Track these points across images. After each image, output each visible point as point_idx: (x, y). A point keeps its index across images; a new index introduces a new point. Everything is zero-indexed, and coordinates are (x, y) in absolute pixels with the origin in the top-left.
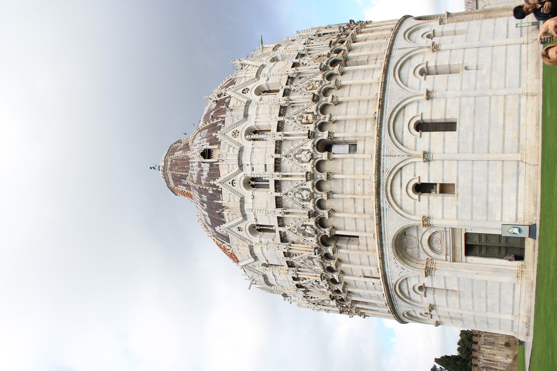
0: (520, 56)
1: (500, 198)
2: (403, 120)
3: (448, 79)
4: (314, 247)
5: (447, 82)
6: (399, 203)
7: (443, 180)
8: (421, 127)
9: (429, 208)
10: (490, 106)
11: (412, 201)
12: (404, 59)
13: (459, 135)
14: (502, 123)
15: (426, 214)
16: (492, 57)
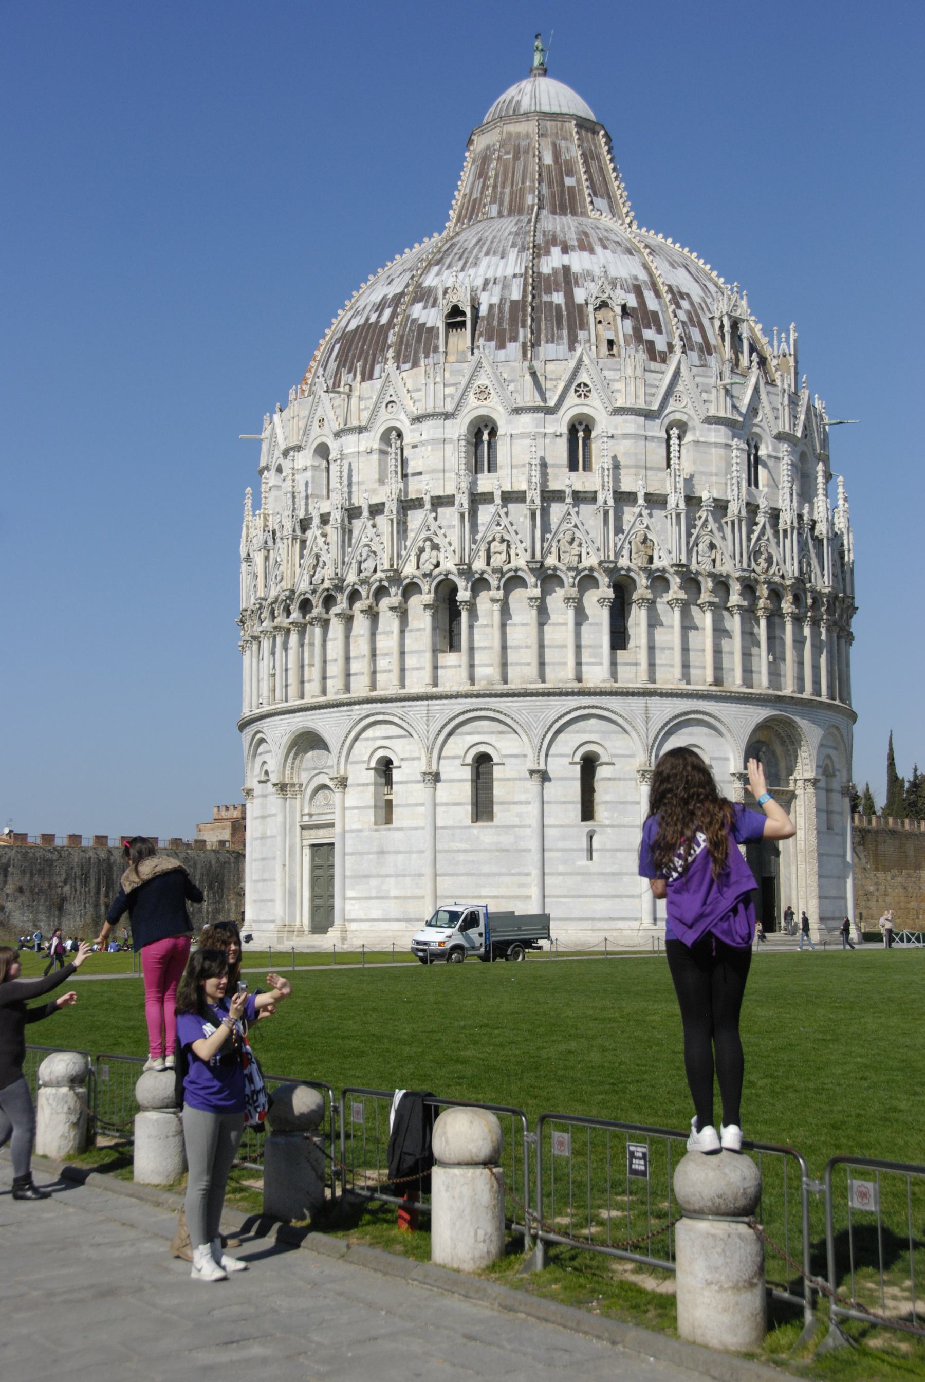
0: (611, 919)
1: (374, 895)
2: (492, 733)
3: (570, 803)
4: (296, 588)
5: (564, 803)
6: (364, 735)
7: (398, 806)
8: (483, 762)
9: (359, 785)
10: (513, 875)
11: (366, 758)
12: (620, 721)
13: (466, 827)
14: (483, 893)
15: (349, 782)
16: (613, 874)
